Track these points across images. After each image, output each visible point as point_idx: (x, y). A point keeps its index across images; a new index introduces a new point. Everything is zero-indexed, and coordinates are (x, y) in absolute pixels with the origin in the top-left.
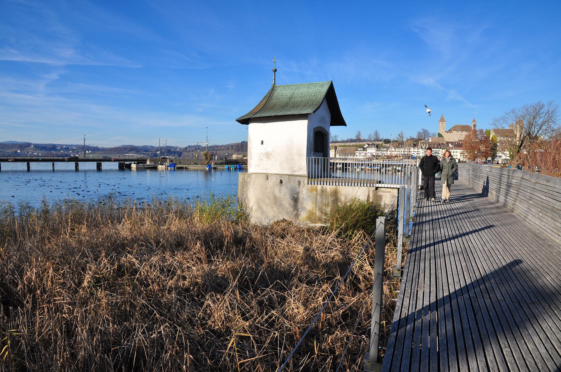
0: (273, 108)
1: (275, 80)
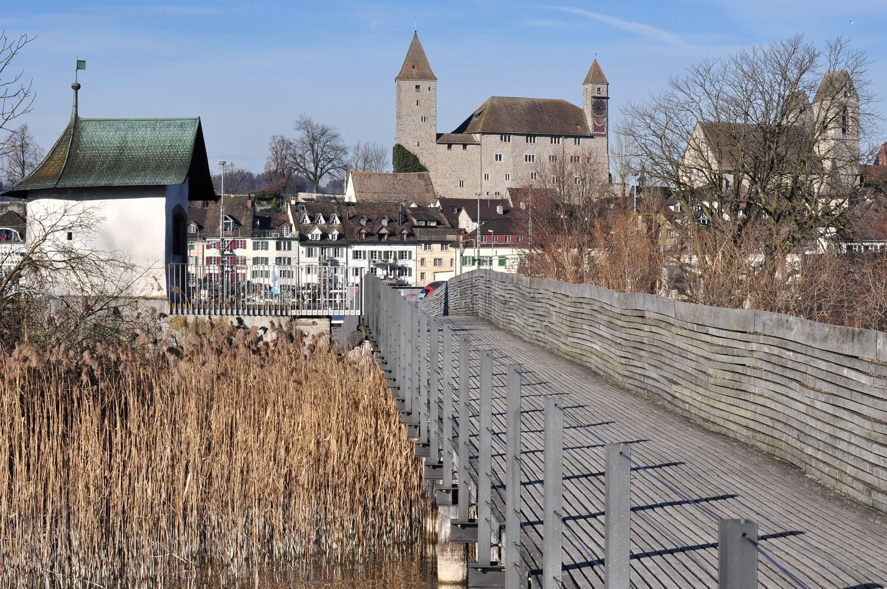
0: (90, 168)
1: (76, 106)
